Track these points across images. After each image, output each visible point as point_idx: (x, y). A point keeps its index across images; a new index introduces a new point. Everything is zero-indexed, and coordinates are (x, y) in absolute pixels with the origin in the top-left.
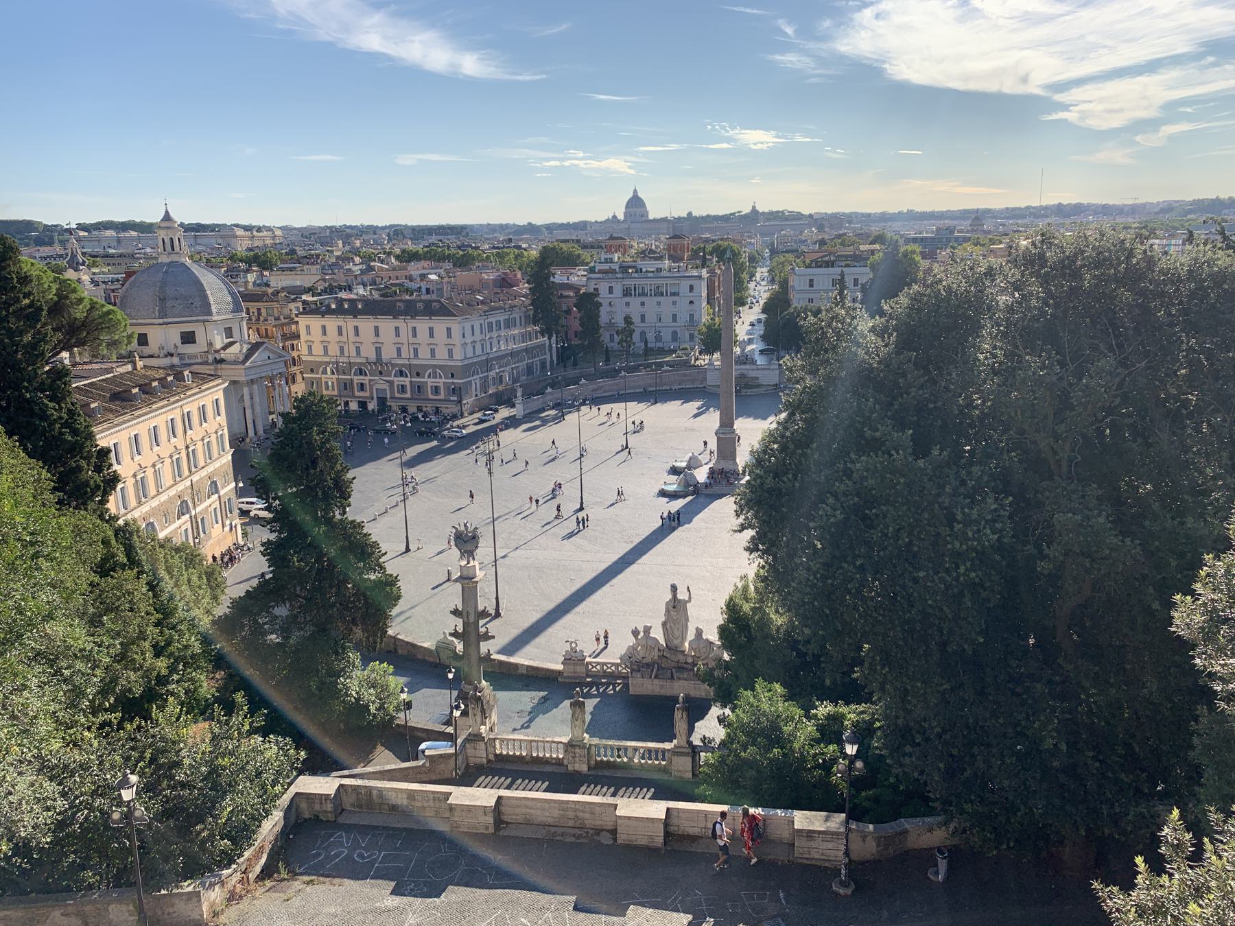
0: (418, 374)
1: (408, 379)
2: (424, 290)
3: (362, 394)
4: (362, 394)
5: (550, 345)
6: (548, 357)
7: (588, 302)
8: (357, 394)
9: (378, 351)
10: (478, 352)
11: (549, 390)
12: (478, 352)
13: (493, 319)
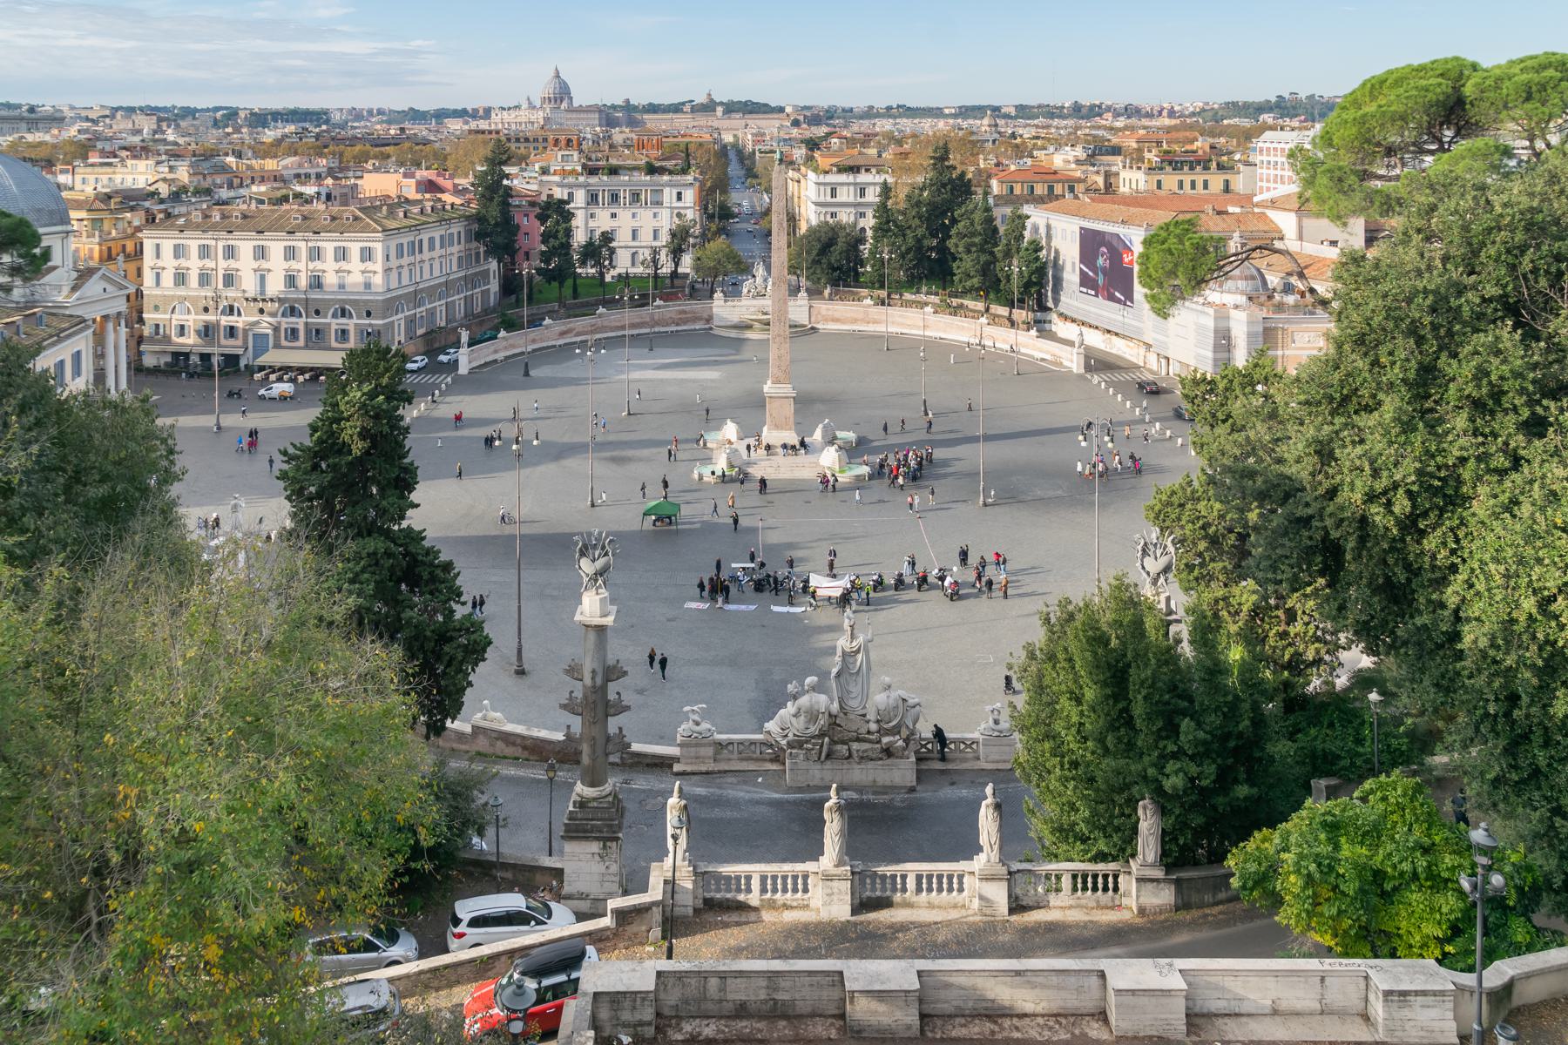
0: (317, 312)
1: (304, 319)
6: (494, 286)
7: (556, 211)
10: (405, 281)
11: (502, 333)
12: (405, 281)
13: (425, 237)
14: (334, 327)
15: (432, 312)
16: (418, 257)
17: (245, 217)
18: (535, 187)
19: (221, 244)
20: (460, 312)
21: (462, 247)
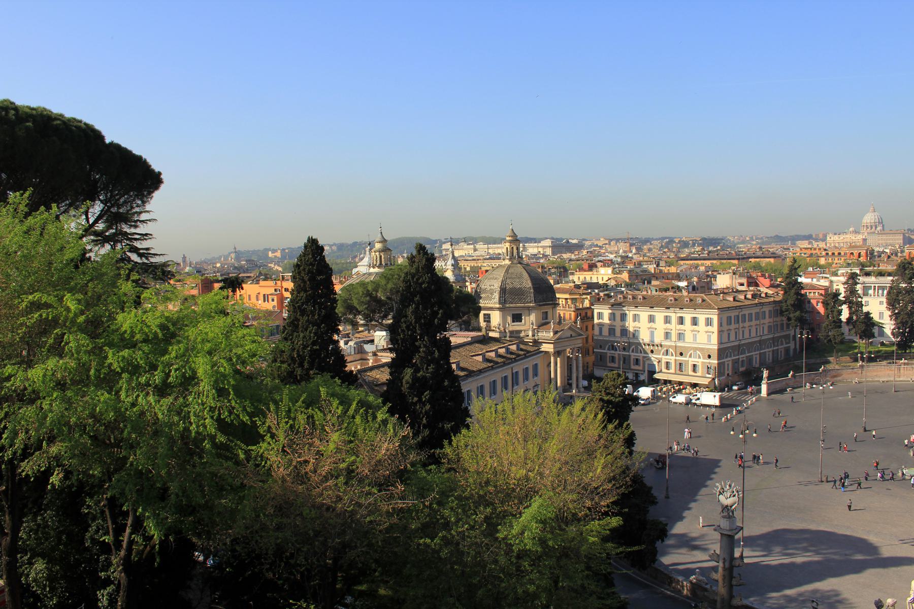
0: (681, 354)
1: (674, 358)
2: (690, 288)
3: (636, 367)
4: (636, 367)
5: (794, 336)
6: (792, 345)
8: (633, 367)
9: (652, 334)
10: (732, 338)
13: (746, 312)
14: (691, 364)
15: (750, 359)
16: (741, 325)
17: (644, 298)
18: (827, 284)
19: (632, 313)
20: (769, 358)
21: (771, 320)
